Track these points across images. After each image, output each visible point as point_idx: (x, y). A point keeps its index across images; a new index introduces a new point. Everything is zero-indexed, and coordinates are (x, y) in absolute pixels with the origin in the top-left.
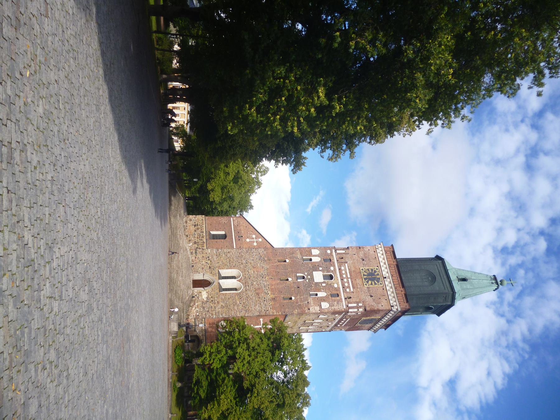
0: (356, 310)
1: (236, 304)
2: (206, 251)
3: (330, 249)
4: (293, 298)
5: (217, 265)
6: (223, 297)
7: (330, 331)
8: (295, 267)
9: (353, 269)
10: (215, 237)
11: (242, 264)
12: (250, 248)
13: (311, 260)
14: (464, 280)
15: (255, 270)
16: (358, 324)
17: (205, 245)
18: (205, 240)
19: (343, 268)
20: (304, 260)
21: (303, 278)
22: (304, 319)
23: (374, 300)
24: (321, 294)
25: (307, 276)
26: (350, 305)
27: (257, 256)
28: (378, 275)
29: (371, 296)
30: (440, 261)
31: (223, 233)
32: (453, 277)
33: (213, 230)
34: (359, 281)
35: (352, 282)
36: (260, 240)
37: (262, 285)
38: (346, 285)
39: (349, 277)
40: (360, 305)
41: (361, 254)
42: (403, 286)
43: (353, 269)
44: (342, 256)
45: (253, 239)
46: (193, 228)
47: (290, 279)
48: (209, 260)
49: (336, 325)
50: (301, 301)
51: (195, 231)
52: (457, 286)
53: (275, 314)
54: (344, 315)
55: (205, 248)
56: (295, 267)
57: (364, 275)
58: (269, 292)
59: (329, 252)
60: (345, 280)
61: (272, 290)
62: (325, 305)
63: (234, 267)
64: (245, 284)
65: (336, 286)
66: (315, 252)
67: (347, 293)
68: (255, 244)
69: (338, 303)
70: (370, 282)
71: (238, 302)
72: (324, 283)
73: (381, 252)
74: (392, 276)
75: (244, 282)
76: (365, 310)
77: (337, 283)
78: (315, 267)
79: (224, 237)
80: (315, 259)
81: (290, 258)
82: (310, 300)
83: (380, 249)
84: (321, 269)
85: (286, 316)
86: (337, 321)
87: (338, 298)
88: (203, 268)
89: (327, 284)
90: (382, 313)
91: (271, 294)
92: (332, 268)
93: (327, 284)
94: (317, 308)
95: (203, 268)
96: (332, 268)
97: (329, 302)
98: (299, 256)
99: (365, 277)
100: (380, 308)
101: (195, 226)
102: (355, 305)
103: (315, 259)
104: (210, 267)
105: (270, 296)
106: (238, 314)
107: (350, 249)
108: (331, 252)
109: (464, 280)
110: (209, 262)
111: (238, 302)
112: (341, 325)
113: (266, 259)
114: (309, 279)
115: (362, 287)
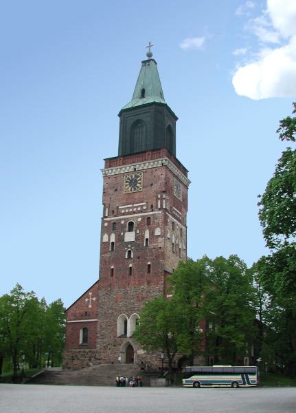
0: (164, 201)
2: (98, 349)
3: (103, 222)
4: (149, 263)
5: (112, 338)
7: (187, 227)
8: (118, 259)
9: (124, 201)
10: (85, 339)
12: (96, 304)
13: (113, 243)
14: (143, 92)
15: (119, 300)
16: (181, 199)
17: (92, 350)
18: (88, 350)
19: (123, 211)
20: (112, 249)
21: (130, 252)
22: (171, 253)
23: (156, 183)
24: (147, 235)
25: (128, 248)
26: (159, 206)
28: (132, 176)
29: (152, 184)
30: (123, 114)
31: (81, 332)
32: (140, 103)
33: (79, 341)
34: (136, 196)
35: (136, 203)
36: (90, 294)
38: (139, 209)
39: (131, 206)
40: (159, 197)
41: (111, 191)
42: (145, 152)
43: (124, 201)
44: (111, 212)
45: (89, 301)
46: (75, 362)
47: (131, 265)
49: (180, 221)
50: (152, 255)
51: (78, 359)
52: (149, 100)
54: (169, 213)
55: (95, 350)
56: (118, 259)
57: (131, 190)
59: (106, 224)
60: (135, 210)
61: (140, 284)
62: (158, 232)
63: (115, 321)
64: (132, 310)
65: (139, 220)
66: (105, 239)
67: (147, 209)
68: (94, 299)
69: (156, 219)
70: (138, 185)
72: (136, 231)
73: (110, 171)
74: (134, 162)
76: (164, 192)
77: (137, 218)
78: (120, 239)
79: (85, 330)
80: (113, 239)
81: (110, 264)
82: (151, 246)
83: (107, 172)
84: (122, 234)
85: (166, 272)
86: (175, 220)
87: (152, 218)
89: (137, 228)
90: (170, 175)
92: (123, 222)
93: (137, 228)
94: (160, 239)
96: (123, 222)
97: (155, 228)
98: (109, 255)
99: (133, 190)
100: (163, 177)
101: (73, 359)
102: (159, 202)
103: (113, 239)
104: (115, 346)
105: (145, 286)
107: (105, 202)
108: (107, 221)
109: (143, 92)
112: (180, 215)
114: (132, 246)
115: (142, 193)
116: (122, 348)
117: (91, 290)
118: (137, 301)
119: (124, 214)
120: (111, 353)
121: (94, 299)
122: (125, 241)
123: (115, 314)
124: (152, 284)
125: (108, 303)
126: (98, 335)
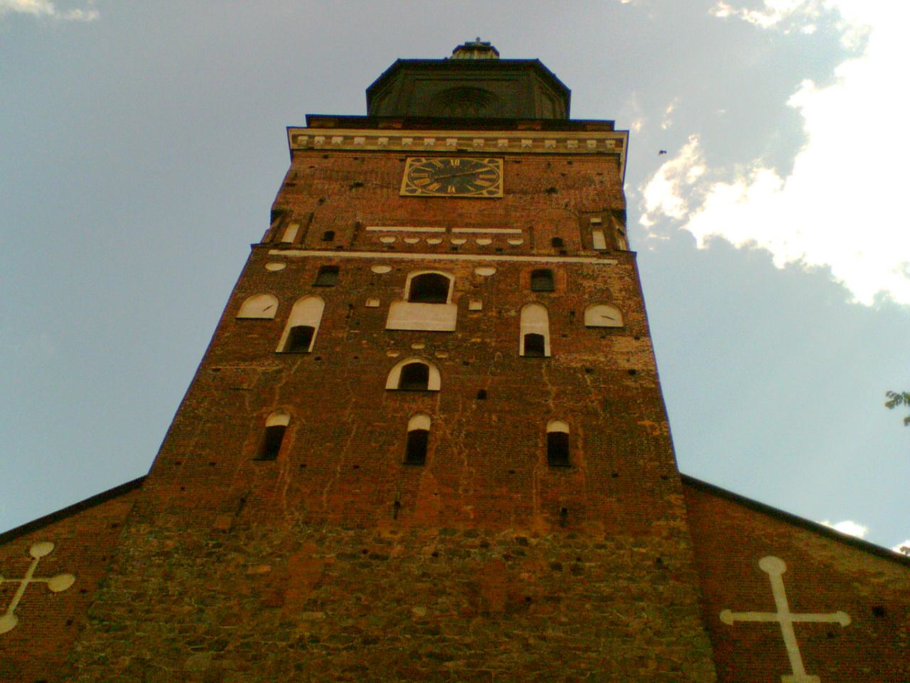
9: (401, 214)
27: (181, 574)
37: (441, 566)
47: (420, 423)
53: (680, 524)
58: (511, 533)
78: (359, 320)
80: (309, 312)
91: (521, 523)
105: (540, 532)
113: (223, 522)
117: (61, 529)
118: (468, 616)
119: (391, 248)
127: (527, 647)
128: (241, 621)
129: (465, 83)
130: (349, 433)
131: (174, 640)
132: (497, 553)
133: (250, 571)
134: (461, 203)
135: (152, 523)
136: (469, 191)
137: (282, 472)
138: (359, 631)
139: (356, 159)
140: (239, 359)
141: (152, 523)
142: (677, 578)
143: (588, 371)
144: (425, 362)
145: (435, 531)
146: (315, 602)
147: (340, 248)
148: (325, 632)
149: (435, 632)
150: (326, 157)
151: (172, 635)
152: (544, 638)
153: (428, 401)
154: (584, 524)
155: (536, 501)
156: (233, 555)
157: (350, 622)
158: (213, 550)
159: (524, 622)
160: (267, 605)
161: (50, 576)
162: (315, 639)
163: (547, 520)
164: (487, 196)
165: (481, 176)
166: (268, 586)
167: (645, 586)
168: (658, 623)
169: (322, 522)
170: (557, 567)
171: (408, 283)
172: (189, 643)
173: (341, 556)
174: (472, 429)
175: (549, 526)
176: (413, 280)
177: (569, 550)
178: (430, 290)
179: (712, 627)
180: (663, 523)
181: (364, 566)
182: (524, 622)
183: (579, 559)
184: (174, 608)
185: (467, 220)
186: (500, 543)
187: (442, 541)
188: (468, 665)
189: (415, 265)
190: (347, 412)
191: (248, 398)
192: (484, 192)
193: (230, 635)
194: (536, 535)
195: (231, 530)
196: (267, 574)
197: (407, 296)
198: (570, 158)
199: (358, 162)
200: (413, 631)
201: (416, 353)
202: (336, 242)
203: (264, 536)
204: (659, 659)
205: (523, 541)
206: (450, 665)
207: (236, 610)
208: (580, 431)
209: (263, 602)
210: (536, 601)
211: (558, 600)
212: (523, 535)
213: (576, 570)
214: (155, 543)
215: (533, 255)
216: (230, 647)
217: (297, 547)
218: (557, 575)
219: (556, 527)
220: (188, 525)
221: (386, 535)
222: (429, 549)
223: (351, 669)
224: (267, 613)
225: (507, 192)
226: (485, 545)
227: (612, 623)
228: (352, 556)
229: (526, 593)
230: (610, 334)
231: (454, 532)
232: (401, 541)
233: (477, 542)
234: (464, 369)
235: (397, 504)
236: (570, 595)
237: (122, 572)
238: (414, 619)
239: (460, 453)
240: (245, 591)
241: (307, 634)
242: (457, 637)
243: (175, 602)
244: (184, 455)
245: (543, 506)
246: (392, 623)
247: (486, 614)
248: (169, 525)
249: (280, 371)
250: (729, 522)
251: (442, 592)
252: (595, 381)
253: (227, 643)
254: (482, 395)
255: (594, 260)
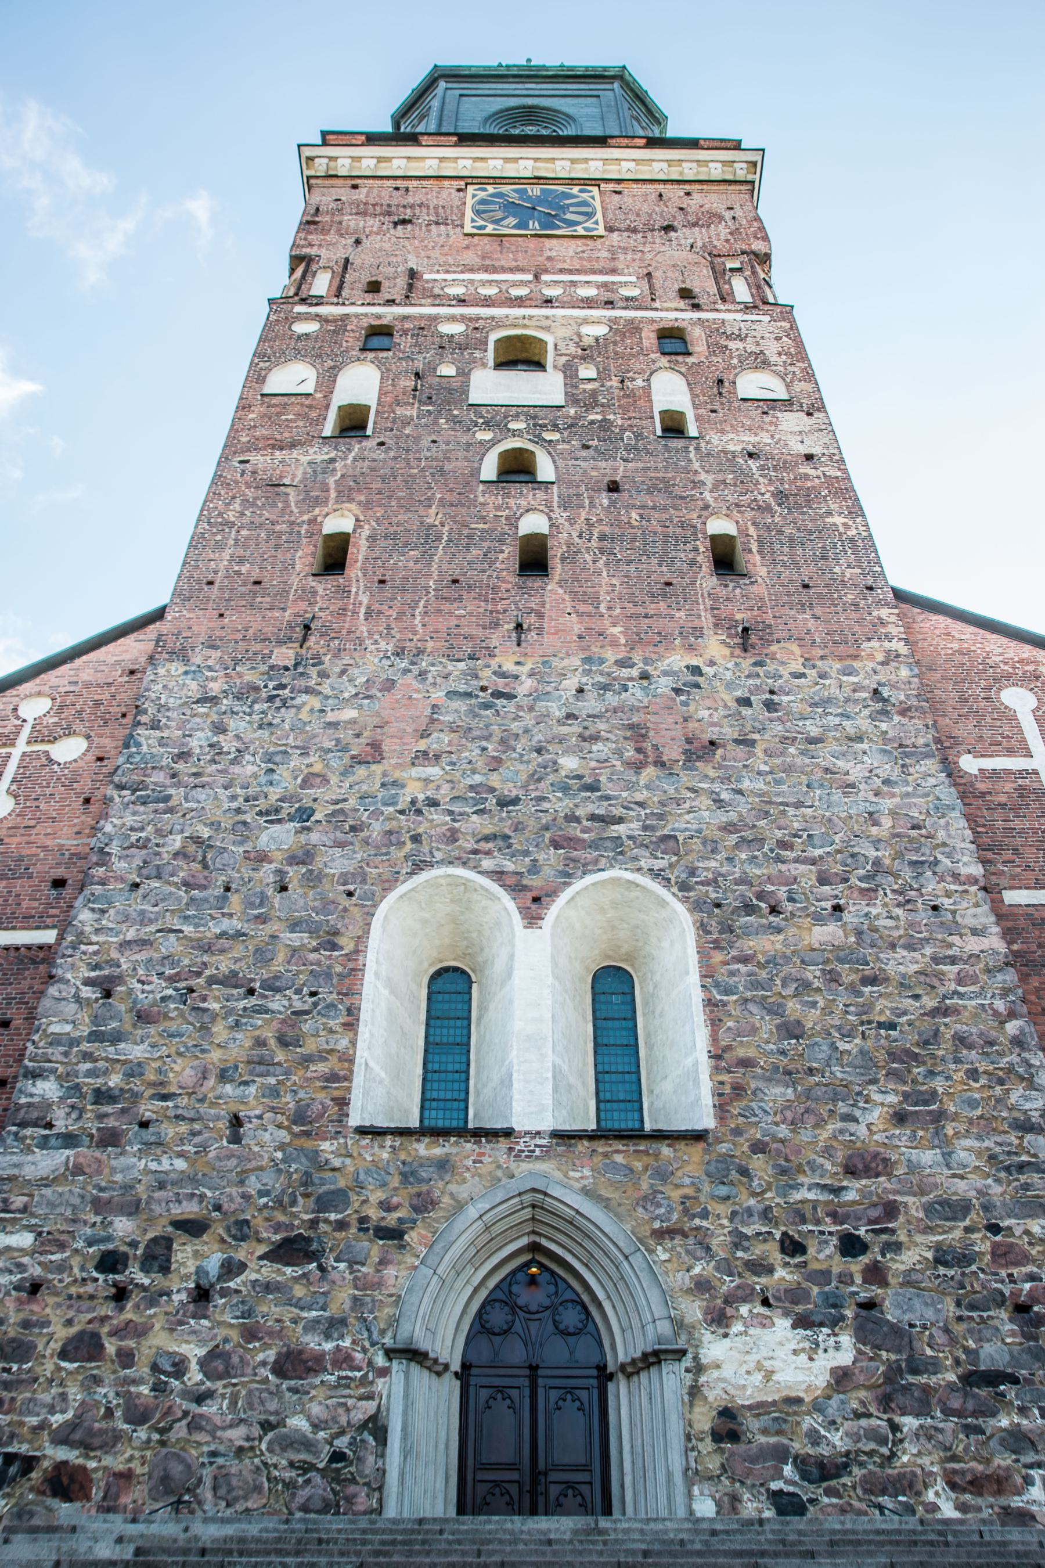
1: (842, 954)
5: (267, 1138)
6: (779, 1093)
11: (303, 857)
27: (237, 725)
37: (591, 704)
47: (533, 523)
48: (158, 1256)
58: (678, 660)
61: (648, 639)
64: (582, 844)
71: (827, 933)
75: (551, 858)
80: (361, 383)
88: (294, 1365)
91: (691, 648)
95: (294, 1365)
104: (292, 1249)
106: (973, 944)
110: (194, 1259)
111: (827, 933)
116: (437, 1296)
120: (217, 1362)
121: (69, 750)
122: (474, 398)
123: (336, 863)
124: (787, 658)
125: (248, 769)
126: (47, 1089)
127: (719, 803)
128: (328, 782)
129: (530, 101)
130: (439, 538)
131: (238, 811)
132: (663, 685)
133: (331, 717)
134: (548, 243)
135: (186, 660)
136: (559, 227)
137: (354, 590)
138: (492, 790)
139: (397, 189)
140: (273, 447)
141: (186, 660)
142: (903, 713)
143: (751, 455)
144: (530, 446)
145: (576, 661)
146: (425, 753)
147: (391, 302)
148: (444, 793)
149: (593, 788)
150: (355, 187)
151: (234, 805)
152: (740, 792)
153: (540, 495)
154: (774, 648)
155: (706, 620)
156: (304, 697)
157: (478, 779)
158: (275, 692)
159: (712, 773)
160: (358, 761)
161: (54, 740)
162: (433, 803)
163: (723, 642)
164: (583, 233)
165: (571, 209)
166: (358, 736)
167: (864, 723)
168: (888, 770)
169: (420, 652)
170: (746, 702)
171: (491, 346)
172: (260, 813)
173: (451, 694)
174: (607, 530)
175: (727, 651)
176: (498, 342)
177: (758, 682)
178: (520, 356)
179: (951, 771)
180: (874, 644)
181: (487, 706)
182: (712, 773)
183: (772, 692)
184: (236, 769)
185: (560, 266)
186: (666, 673)
187: (587, 673)
188: (645, 828)
189: (498, 323)
190: (433, 510)
191: (293, 496)
192: (579, 228)
193: (315, 800)
194: (712, 663)
195: (296, 665)
196: (353, 722)
197: (491, 363)
198: (687, 187)
199: (402, 192)
200: (565, 789)
201: (515, 433)
202: (385, 295)
203: (343, 672)
204: (893, 813)
205: (696, 670)
206: (620, 829)
207: (318, 768)
208: (752, 531)
209: (353, 757)
210: (724, 746)
211: (752, 743)
212: (695, 662)
213: (770, 706)
214: (194, 685)
215: (656, 309)
216: (318, 816)
217: (389, 685)
218: (746, 712)
219: (738, 651)
220: (236, 662)
221: (509, 667)
222: (571, 683)
223: (487, 838)
224: (361, 771)
225: (610, 229)
226: (645, 676)
227: (827, 770)
228: (469, 695)
229: (707, 737)
230: (774, 409)
231: (602, 661)
232: (531, 675)
233: (635, 673)
234: (584, 453)
235: (519, 626)
236: (766, 737)
237: (155, 726)
238: (563, 773)
239: (594, 562)
240: (329, 744)
241: (421, 797)
242: (625, 794)
243: (234, 762)
244: (216, 572)
245: (716, 625)
246: (536, 778)
247: (660, 764)
248: (210, 663)
249: (332, 461)
250: (956, 646)
251: (595, 738)
252: (762, 468)
253: (313, 812)
254: (613, 487)
255: (739, 316)
